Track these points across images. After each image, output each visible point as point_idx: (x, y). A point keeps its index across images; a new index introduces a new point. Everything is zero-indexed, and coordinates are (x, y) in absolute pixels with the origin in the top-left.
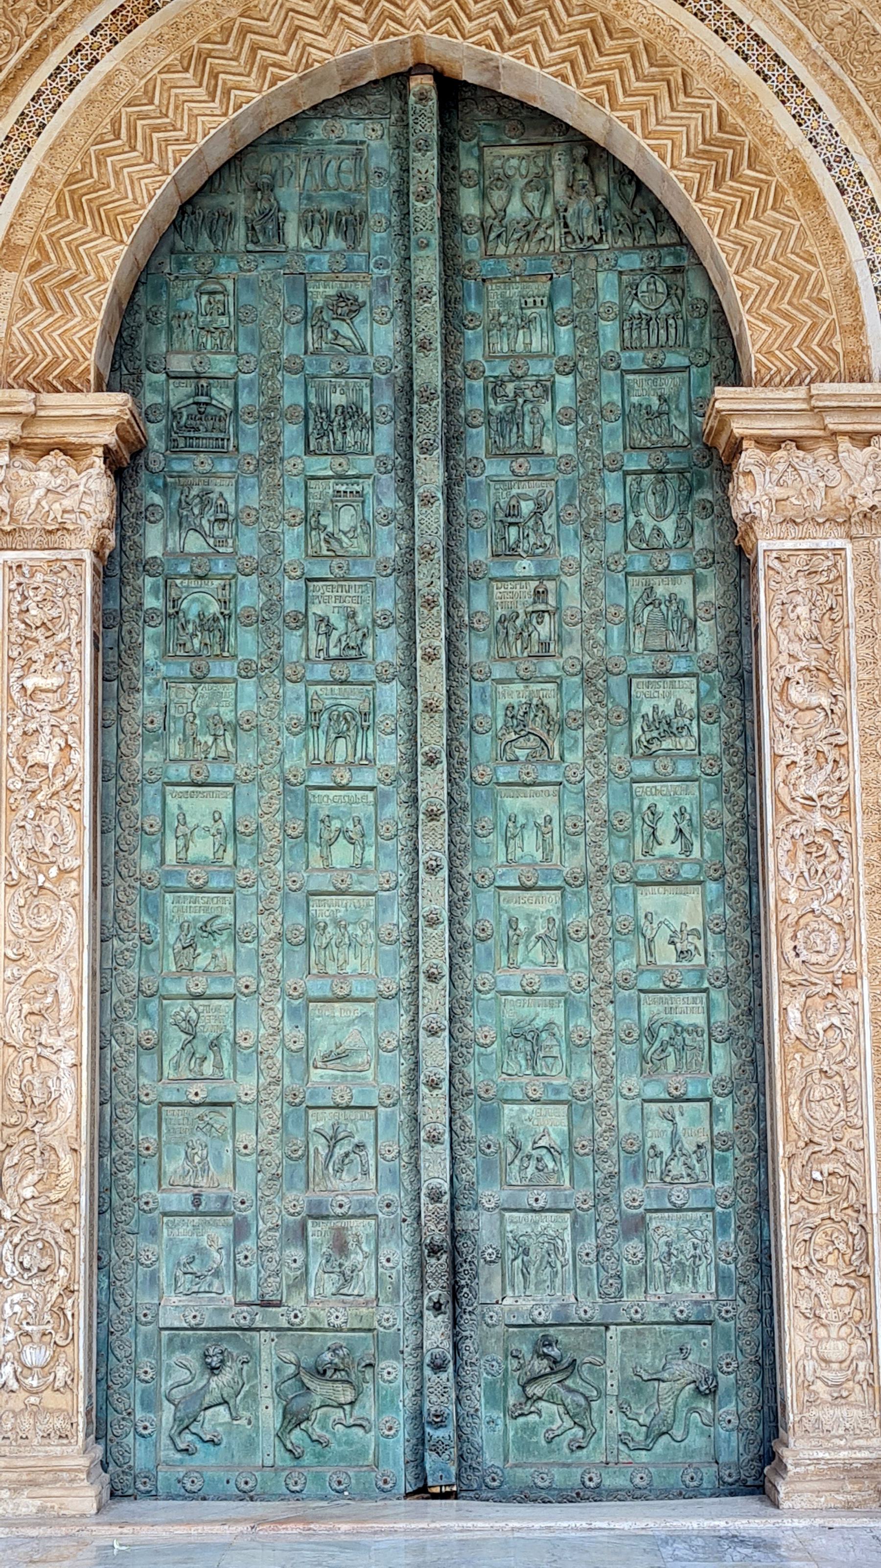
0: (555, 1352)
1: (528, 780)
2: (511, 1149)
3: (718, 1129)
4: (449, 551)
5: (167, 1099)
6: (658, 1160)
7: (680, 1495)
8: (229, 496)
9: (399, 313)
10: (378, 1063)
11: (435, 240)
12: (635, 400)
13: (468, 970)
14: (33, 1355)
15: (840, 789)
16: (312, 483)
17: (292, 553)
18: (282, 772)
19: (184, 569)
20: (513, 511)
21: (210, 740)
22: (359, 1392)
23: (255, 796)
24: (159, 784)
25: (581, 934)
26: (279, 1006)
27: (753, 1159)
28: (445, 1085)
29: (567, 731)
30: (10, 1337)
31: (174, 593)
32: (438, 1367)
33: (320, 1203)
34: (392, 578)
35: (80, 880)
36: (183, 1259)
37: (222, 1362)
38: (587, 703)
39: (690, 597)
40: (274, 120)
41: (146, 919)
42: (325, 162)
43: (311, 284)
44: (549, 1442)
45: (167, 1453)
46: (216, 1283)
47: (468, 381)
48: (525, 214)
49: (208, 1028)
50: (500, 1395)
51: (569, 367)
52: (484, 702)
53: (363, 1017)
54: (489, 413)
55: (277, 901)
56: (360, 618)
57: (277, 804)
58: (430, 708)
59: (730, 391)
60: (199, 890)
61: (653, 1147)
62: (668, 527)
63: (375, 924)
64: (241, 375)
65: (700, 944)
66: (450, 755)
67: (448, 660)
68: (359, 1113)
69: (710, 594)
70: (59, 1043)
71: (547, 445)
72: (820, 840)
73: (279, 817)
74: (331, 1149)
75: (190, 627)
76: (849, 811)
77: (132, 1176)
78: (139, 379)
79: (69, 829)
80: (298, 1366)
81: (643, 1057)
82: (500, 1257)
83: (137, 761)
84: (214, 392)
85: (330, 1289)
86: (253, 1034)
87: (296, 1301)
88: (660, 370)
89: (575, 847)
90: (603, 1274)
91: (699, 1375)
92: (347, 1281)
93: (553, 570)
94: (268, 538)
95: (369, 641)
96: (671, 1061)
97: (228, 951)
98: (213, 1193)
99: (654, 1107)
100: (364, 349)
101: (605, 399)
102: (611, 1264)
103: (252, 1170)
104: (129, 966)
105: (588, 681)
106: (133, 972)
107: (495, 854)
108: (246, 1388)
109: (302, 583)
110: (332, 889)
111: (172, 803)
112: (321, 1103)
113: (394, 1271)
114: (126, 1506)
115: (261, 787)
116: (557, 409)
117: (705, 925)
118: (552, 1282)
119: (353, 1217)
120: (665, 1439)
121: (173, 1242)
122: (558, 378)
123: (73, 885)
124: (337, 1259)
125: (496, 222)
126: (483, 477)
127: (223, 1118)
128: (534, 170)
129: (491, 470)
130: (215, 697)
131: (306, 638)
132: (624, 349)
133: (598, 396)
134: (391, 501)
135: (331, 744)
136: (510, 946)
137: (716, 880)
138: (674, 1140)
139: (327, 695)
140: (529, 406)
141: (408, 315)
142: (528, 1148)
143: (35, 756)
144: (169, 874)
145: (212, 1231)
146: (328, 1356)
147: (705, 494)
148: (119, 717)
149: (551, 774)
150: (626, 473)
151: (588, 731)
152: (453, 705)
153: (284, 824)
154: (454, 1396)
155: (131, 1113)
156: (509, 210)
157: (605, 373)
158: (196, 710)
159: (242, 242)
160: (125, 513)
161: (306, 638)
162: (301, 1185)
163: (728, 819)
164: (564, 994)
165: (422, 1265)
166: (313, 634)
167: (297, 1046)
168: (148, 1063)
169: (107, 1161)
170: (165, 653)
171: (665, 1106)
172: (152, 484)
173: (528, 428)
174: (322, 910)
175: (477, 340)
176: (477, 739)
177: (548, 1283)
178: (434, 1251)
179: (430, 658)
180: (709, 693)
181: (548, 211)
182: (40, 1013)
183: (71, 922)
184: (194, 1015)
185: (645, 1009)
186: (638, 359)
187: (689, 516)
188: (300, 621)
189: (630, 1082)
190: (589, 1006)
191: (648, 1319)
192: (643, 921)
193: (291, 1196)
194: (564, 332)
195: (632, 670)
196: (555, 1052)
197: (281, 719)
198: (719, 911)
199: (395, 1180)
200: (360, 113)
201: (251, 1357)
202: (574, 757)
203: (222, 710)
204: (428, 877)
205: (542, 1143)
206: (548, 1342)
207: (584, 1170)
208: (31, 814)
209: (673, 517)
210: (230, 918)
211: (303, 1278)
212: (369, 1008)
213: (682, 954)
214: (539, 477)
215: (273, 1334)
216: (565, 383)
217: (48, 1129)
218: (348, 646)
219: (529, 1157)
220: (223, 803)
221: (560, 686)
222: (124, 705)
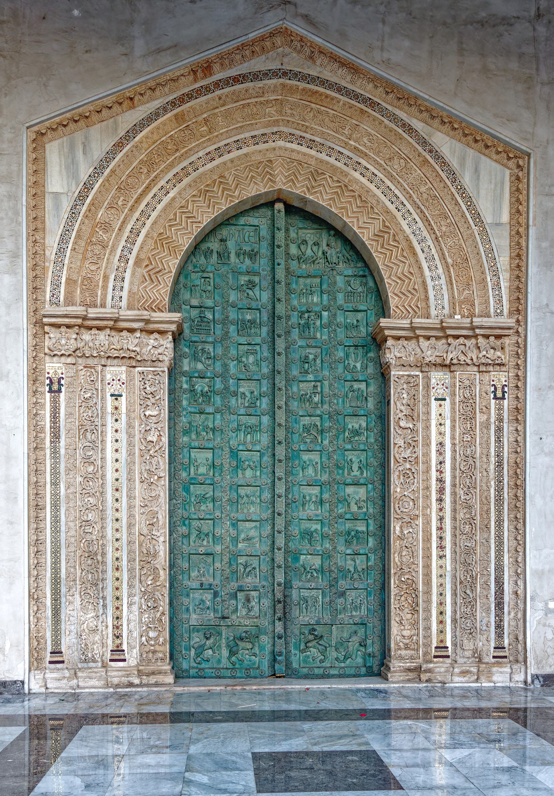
2: (303, 569)
3: (370, 564)
5: (192, 552)
8: (211, 350)
9: (270, 287)
11: (283, 262)
12: (348, 321)
14: (152, 634)
15: (414, 455)
16: (240, 346)
19: (196, 375)
20: (307, 357)
21: (205, 434)
29: (324, 434)
30: (144, 628)
35: (165, 480)
39: (365, 389)
40: (228, 216)
41: (184, 493)
46: (208, 611)
48: (313, 254)
50: (298, 646)
53: (256, 527)
56: (255, 393)
57: (228, 456)
60: (201, 484)
62: (358, 365)
63: (260, 496)
65: (365, 505)
68: (254, 558)
69: (372, 389)
70: (159, 534)
71: (318, 335)
72: (408, 472)
73: (228, 460)
74: (245, 569)
76: (417, 463)
77: (181, 577)
78: (180, 308)
79: (161, 463)
81: (346, 541)
83: (181, 440)
84: (206, 313)
89: (326, 472)
93: (320, 378)
94: (225, 366)
95: (259, 401)
97: (211, 504)
98: (207, 583)
99: (349, 557)
101: (338, 320)
102: (334, 606)
103: (219, 576)
104: (179, 509)
105: (330, 417)
106: (180, 511)
107: (298, 474)
109: (236, 381)
111: (192, 455)
114: (181, 680)
115: (222, 450)
117: (367, 499)
121: (194, 599)
122: (323, 312)
123: (163, 483)
127: (210, 559)
128: (316, 239)
129: (300, 344)
130: (206, 419)
131: (237, 400)
134: (266, 354)
135: (245, 436)
136: (303, 505)
138: (355, 568)
139: (244, 419)
141: (273, 288)
142: (308, 569)
143: (149, 438)
144: (192, 479)
145: (206, 595)
146: (244, 635)
147: (371, 355)
148: (175, 425)
149: (318, 448)
150: (345, 346)
151: (331, 434)
153: (230, 463)
155: (180, 556)
156: (307, 252)
157: (339, 312)
161: (237, 400)
162: (235, 580)
165: (274, 606)
166: (240, 399)
168: (185, 541)
169: (172, 572)
170: (190, 403)
171: (352, 556)
172: (185, 345)
173: (312, 329)
174: (242, 491)
175: (295, 297)
176: (294, 435)
179: (279, 408)
180: (371, 422)
181: (320, 253)
182: (152, 524)
183: (162, 494)
185: (347, 525)
186: (350, 306)
188: (235, 394)
189: (341, 548)
193: (232, 584)
194: (325, 297)
196: (318, 539)
198: (372, 494)
200: (257, 215)
201: (220, 634)
202: (326, 442)
207: (326, 576)
208: (148, 458)
210: (212, 493)
212: (258, 524)
213: (359, 508)
214: (315, 347)
216: (325, 314)
217: (155, 562)
220: (209, 455)
221: (321, 418)
222: (176, 421)
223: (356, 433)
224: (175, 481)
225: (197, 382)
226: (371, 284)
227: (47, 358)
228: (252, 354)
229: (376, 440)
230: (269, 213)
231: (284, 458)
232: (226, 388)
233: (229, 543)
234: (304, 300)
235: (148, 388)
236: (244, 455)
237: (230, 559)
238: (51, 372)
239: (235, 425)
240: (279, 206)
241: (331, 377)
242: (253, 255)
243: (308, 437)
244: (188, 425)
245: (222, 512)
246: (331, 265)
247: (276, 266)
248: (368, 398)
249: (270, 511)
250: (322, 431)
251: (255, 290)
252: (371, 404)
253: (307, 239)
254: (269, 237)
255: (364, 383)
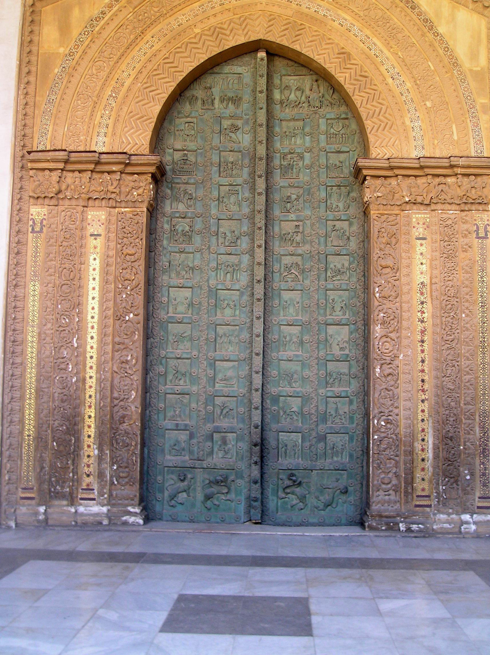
0: (294, 478)
1: (291, 288)
4: (266, 211)
5: (168, 391)
6: (331, 417)
7: (334, 525)
8: (193, 191)
10: (238, 382)
11: (265, 106)
12: (331, 162)
13: (269, 352)
16: (220, 187)
17: (214, 211)
18: (208, 284)
19: (177, 215)
21: (184, 273)
22: (229, 489)
23: (199, 292)
24: (167, 288)
25: (307, 341)
26: (205, 362)
27: (362, 418)
28: (260, 390)
31: (173, 223)
32: (256, 482)
33: (217, 427)
34: (247, 220)
36: (172, 444)
37: (185, 478)
38: (312, 263)
42: (228, 80)
43: (222, 120)
44: (292, 507)
45: (166, 506)
47: (275, 154)
48: (296, 99)
49: (183, 369)
51: (310, 150)
52: (277, 262)
53: (234, 367)
54: (282, 165)
55: (205, 327)
56: (236, 233)
57: (206, 295)
58: (259, 264)
59: (364, 161)
61: (330, 412)
62: (341, 205)
64: (198, 150)
65: (347, 346)
66: (265, 280)
67: (265, 248)
69: (355, 228)
74: (222, 410)
75: (179, 235)
77: (156, 417)
80: (209, 480)
82: (278, 447)
83: (160, 279)
85: (220, 455)
86: (197, 371)
87: (209, 459)
88: (339, 152)
89: (306, 311)
90: (311, 454)
91: (341, 487)
92: (226, 453)
93: (302, 218)
95: (239, 241)
96: (337, 384)
100: (240, 143)
101: (321, 161)
104: (156, 347)
107: (279, 314)
108: (192, 487)
109: (217, 220)
110: (224, 324)
112: (219, 395)
113: (242, 451)
115: (201, 289)
116: (305, 164)
117: (349, 339)
118: (294, 456)
119: (229, 432)
120: (329, 507)
124: (223, 447)
125: (286, 101)
126: (279, 187)
129: (281, 184)
131: (218, 239)
132: (328, 144)
133: (318, 160)
134: (247, 195)
137: (353, 324)
138: (337, 409)
140: (295, 163)
141: (255, 131)
143: (128, 276)
147: (353, 194)
151: (312, 273)
152: (267, 263)
154: (260, 492)
157: (321, 152)
158: (180, 262)
159: (200, 106)
160: (158, 196)
161: (218, 239)
163: (359, 304)
164: (301, 361)
166: (220, 238)
167: (212, 376)
171: (333, 399)
172: (167, 187)
173: (294, 170)
174: (220, 330)
177: (293, 456)
178: (256, 445)
179: (259, 246)
181: (303, 98)
184: (177, 365)
185: (328, 367)
187: (348, 202)
190: (309, 365)
191: (326, 468)
192: (329, 338)
195: (327, 253)
197: (209, 266)
199: (243, 421)
200: (239, 63)
203: (189, 263)
204: (256, 320)
205: (292, 410)
206: (293, 475)
209: (343, 202)
210: (190, 333)
211: (211, 453)
213: (342, 349)
214: (298, 187)
215: (202, 470)
216: (307, 155)
218: (231, 242)
219: (288, 415)
221: (303, 258)
222: (156, 260)
223: (339, 272)
224: (153, 319)
225: (178, 222)
226: (354, 126)
227: (32, 200)
228: (233, 194)
229: (359, 279)
230: (253, 61)
231: (263, 297)
232: (207, 228)
233: (206, 383)
234: (286, 142)
235: (127, 228)
236: (222, 293)
237: (206, 399)
238: (34, 214)
239: (214, 264)
240: (262, 54)
241: (313, 217)
242: (236, 101)
243: (289, 276)
244: (168, 264)
245: (199, 352)
246: (313, 109)
247: (258, 111)
248: (351, 237)
249: (248, 351)
250: (303, 271)
251: (237, 133)
252: (353, 245)
253: (291, 85)
254: (252, 84)
255: (347, 222)
